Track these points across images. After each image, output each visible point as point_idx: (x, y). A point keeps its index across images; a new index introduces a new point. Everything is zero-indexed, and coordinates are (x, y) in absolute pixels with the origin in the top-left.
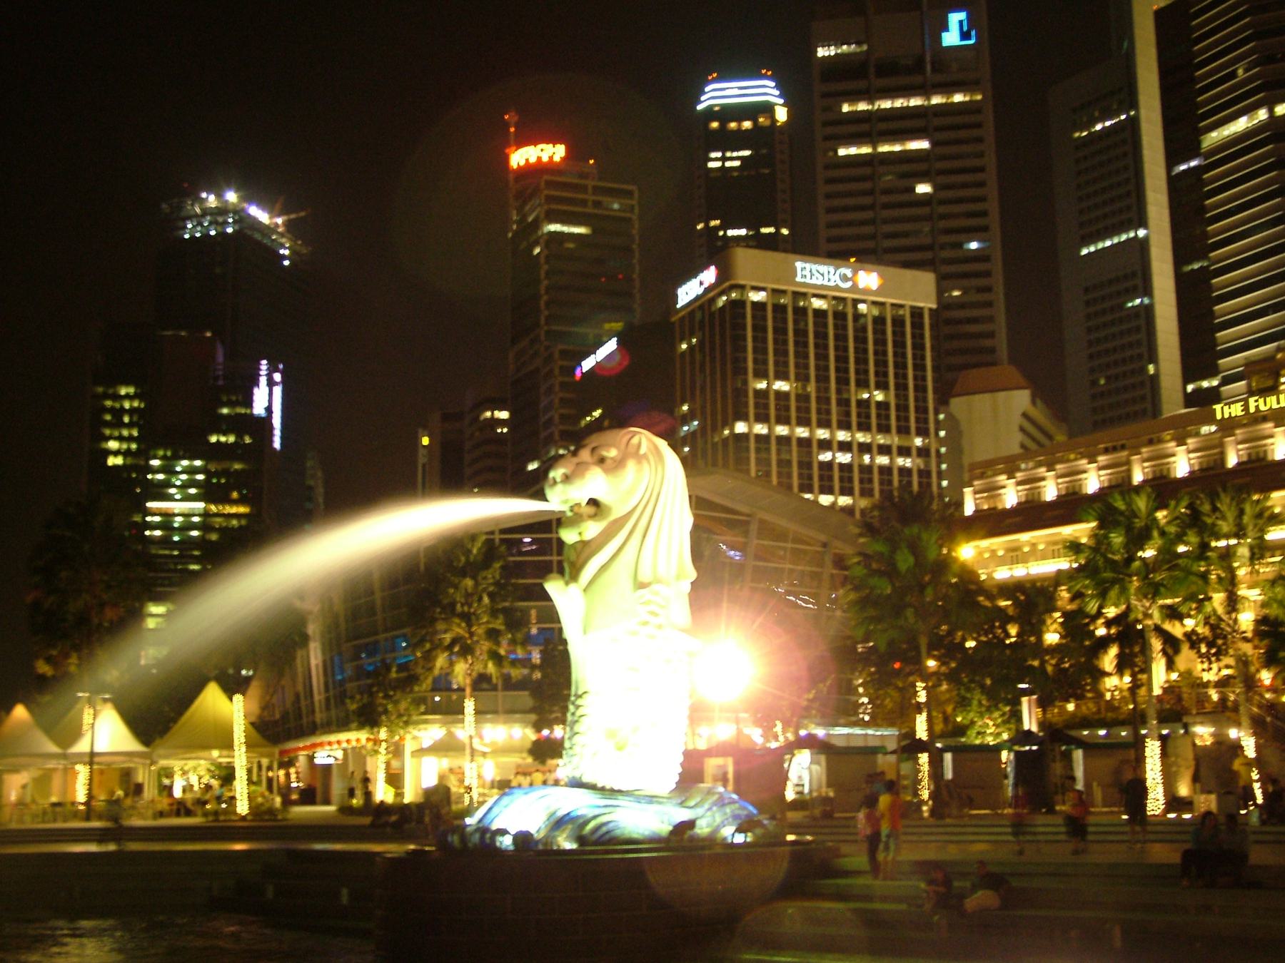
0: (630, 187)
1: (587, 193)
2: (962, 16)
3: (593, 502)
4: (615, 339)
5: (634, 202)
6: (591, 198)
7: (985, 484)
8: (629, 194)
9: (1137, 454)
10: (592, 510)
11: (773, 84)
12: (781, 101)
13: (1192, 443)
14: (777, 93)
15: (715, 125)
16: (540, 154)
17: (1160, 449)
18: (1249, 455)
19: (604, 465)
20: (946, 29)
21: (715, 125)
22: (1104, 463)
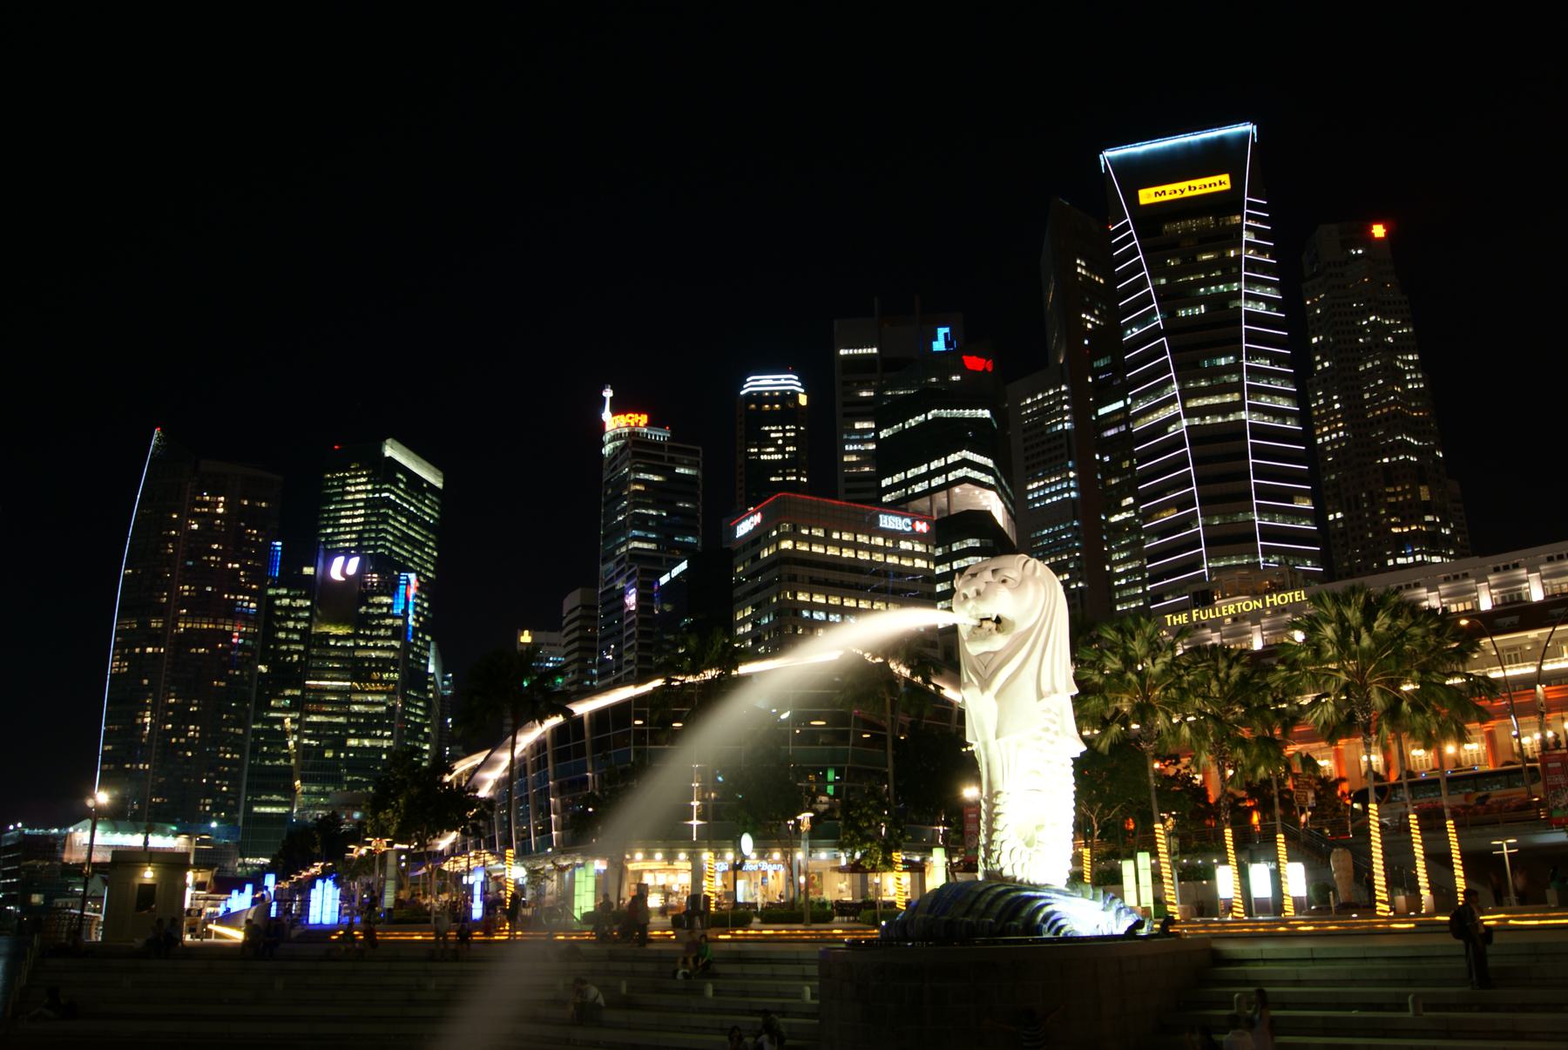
0: (700, 448)
1: (664, 451)
2: (947, 330)
3: (998, 620)
4: (686, 561)
5: (699, 459)
6: (666, 455)
7: (1273, 621)
8: (696, 453)
9: (1483, 582)
10: (994, 626)
11: (796, 378)
12: (802, 390)
13: (1443, 589)
14: (799, 384)
15: (753, 406)
16: (629, 421)
17: (1463, 586)
18: (1503, 598)
19: (1007, 584)
20: (936, 339)
21: (753, 406)
22: (1267, 625)
